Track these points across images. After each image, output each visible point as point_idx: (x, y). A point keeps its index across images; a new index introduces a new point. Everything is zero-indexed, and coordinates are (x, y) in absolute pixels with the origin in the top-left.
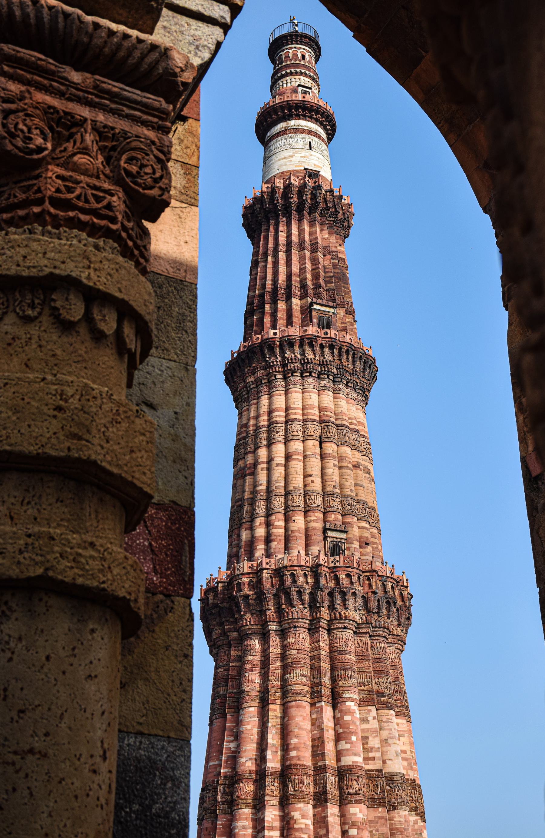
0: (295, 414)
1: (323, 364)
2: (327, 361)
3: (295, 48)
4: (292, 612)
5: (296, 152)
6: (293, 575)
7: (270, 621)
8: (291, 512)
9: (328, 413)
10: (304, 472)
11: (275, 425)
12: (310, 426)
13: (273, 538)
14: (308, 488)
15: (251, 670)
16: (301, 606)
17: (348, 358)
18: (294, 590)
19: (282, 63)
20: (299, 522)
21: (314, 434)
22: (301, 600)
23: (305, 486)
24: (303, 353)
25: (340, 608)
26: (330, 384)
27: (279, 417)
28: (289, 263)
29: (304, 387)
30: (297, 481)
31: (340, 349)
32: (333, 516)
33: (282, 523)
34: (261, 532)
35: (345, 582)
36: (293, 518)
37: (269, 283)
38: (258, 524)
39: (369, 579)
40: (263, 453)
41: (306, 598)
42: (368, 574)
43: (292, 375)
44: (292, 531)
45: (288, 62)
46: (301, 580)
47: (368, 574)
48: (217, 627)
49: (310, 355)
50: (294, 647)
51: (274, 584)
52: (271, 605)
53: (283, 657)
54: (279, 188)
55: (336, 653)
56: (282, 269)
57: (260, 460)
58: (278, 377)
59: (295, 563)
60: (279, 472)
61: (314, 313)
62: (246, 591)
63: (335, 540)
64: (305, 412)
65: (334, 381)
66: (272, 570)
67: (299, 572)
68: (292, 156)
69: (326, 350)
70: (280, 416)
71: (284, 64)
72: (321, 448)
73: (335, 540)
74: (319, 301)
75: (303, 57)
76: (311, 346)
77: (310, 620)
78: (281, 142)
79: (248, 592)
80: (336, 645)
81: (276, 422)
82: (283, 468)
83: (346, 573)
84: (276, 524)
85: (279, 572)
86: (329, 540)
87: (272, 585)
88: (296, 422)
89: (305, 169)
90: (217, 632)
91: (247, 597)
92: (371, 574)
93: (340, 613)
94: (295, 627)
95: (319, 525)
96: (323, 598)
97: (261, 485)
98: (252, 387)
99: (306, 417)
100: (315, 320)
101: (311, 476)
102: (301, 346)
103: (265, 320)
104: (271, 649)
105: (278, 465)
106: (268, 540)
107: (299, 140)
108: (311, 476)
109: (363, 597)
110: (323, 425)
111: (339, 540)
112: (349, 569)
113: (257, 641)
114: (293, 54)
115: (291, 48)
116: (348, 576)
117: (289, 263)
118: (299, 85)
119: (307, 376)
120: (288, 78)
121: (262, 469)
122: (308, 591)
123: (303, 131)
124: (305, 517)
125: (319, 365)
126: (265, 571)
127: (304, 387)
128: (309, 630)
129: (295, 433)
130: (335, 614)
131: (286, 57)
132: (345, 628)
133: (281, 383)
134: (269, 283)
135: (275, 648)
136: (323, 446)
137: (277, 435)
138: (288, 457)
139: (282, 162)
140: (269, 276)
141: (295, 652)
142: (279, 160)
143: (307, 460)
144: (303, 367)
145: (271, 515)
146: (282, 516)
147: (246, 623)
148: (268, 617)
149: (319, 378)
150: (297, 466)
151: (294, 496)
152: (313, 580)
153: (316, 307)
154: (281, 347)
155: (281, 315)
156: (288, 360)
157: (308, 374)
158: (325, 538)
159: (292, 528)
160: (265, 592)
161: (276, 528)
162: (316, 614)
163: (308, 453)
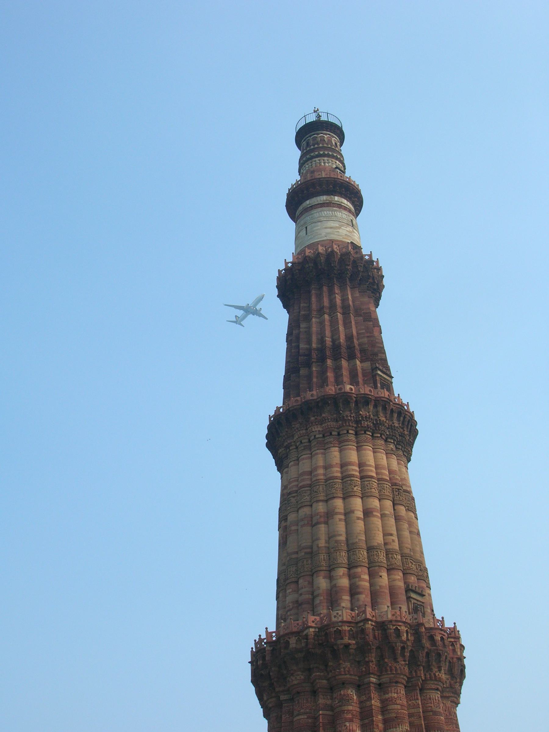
0: (371, 471)
1: (392, 429)
2: (394, 426)
3: (329, 135)
4: (396, 667)
5: (342, 226)
6: (397, 630)
7: (372, 673)
8: (377, 568)
9: (398, 477)
10: (383, 530)
11: (352, 478)
12: (385, 485)
13: (361, 590)
14: (389, 547)
15: (351, 720)
16: (403, 663)
17: (408, 428)
18: (399, 645)
19: (318, 144)
20: (384, 579)
21: (389, 494)
22: (403, 656)
23: (385, 544)
24: (377, 414)
25: (435, 670)
26: (394, 449)
27: (354, 470)
28: (347, 324)
29: (376, 447)
30: (379, 539)
31: (404, 417)
32: (413, 578)
33: (367, 577)
34: (344, 582)
35: (440, 643)
36: (380, 574)
37: (328, 340)
38: (341, 574)
39: (453, 645)
40: (339, 504)
41: (407, 654)
42: (453, 640)
43: (365, 433)
44: (380, 586)
45: (325, 145)
46: (404, 637)
47: (453, 640)
48: (299, 673)
49: (382, 417)
50: (398, 702)
51: (377, 636)
52: (373, 657)
53: (384, 710)
54: (337, 253)
55: (431, 713)
56: (341, 328)
57: (337, 510)
58: (351, 432)
59: (399, 619)
60: (360, 525)
61: (378, 378)
62: (346, 640)
63: (416, 602)
64: (379, 471)
65: (396, 448)
66: (376, 622)
67: (403, 628)
68: (339, 228)
69: (395, 415)
70: (356, 471)
71: (321, 145)
72: (394, 510)
73: (416, 602)
74: (381, 367)
75: (336, 144)
76: (384, 408)
77: (408, 678)
78: (326, 212)
79: (350, 641)
80: (430, 705)
81: (353, 476)
82: (363, 522)
83: (441, 635)
84: (363, 576)
85: (382, 626)
86: (412, 602)
87: (375, 637)
88: (373, 480)
89: (352, 243)
90: (298, 677)
91: (347, 646)
92: (456, 640)
93: (435, 675)
94: (397, 682)
95: (401, 584)
96: (422, 656)
97: (341, 535)
98: (317, 436)
99: (380, 477)
100: (379, 385)
101: (391, 535)
102: (375, 406)
103: (329, 374)
104: (373, 701)
105: (358, 518)
106: (354, 592)
107: (344, 216)
108: (391, 535)
109: (450, 662)
110: (394, 487)
111: (419, 603)
112: (443, 632)
113: (354, 691)
114: (328, 140)
115: (326, 134)
116: (442, 638)
117: (347, 324)
118: (337, 168)
119: (378, 437)
120: (326, 158)
121: (340, 520)
122: (410, 648)
123: (345, 209)
124: (388, 575)
125: (388, 428)
126: (370, 622)
127: (376, 447)
128: (405, 687)
129: (373, 490)
130: (430, 674)
131: (321, 140)
132: (437, 689)
133: (352, 437)
134: (328, 340)
135: (376, 703)
136: (396, 508)
137: (355, 488)
138: (367, 513)
139: (329, 230)
140: (328, 333)
141: (399, 707)
142: (326, 228)
143: (386, 518)
144: (375, 427)
145: (356, 567)
146: (366, 570)
147: (344, 671)
148: (371, 668)
149: (386, 441)
150: (377, 522)
151: (379, 552)
152: (412, 638)
153: (379, 372)
154: (356, 402)
155: (345, 373)
156: (362, 417)
157: (379, 435)
158: (409, 598)
159: (381, 584)
160: (371, 643)
161: (363, 581)
162: (416, 672)
163: (387, 512)
